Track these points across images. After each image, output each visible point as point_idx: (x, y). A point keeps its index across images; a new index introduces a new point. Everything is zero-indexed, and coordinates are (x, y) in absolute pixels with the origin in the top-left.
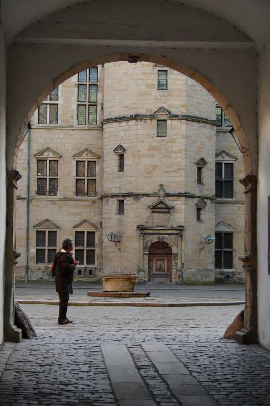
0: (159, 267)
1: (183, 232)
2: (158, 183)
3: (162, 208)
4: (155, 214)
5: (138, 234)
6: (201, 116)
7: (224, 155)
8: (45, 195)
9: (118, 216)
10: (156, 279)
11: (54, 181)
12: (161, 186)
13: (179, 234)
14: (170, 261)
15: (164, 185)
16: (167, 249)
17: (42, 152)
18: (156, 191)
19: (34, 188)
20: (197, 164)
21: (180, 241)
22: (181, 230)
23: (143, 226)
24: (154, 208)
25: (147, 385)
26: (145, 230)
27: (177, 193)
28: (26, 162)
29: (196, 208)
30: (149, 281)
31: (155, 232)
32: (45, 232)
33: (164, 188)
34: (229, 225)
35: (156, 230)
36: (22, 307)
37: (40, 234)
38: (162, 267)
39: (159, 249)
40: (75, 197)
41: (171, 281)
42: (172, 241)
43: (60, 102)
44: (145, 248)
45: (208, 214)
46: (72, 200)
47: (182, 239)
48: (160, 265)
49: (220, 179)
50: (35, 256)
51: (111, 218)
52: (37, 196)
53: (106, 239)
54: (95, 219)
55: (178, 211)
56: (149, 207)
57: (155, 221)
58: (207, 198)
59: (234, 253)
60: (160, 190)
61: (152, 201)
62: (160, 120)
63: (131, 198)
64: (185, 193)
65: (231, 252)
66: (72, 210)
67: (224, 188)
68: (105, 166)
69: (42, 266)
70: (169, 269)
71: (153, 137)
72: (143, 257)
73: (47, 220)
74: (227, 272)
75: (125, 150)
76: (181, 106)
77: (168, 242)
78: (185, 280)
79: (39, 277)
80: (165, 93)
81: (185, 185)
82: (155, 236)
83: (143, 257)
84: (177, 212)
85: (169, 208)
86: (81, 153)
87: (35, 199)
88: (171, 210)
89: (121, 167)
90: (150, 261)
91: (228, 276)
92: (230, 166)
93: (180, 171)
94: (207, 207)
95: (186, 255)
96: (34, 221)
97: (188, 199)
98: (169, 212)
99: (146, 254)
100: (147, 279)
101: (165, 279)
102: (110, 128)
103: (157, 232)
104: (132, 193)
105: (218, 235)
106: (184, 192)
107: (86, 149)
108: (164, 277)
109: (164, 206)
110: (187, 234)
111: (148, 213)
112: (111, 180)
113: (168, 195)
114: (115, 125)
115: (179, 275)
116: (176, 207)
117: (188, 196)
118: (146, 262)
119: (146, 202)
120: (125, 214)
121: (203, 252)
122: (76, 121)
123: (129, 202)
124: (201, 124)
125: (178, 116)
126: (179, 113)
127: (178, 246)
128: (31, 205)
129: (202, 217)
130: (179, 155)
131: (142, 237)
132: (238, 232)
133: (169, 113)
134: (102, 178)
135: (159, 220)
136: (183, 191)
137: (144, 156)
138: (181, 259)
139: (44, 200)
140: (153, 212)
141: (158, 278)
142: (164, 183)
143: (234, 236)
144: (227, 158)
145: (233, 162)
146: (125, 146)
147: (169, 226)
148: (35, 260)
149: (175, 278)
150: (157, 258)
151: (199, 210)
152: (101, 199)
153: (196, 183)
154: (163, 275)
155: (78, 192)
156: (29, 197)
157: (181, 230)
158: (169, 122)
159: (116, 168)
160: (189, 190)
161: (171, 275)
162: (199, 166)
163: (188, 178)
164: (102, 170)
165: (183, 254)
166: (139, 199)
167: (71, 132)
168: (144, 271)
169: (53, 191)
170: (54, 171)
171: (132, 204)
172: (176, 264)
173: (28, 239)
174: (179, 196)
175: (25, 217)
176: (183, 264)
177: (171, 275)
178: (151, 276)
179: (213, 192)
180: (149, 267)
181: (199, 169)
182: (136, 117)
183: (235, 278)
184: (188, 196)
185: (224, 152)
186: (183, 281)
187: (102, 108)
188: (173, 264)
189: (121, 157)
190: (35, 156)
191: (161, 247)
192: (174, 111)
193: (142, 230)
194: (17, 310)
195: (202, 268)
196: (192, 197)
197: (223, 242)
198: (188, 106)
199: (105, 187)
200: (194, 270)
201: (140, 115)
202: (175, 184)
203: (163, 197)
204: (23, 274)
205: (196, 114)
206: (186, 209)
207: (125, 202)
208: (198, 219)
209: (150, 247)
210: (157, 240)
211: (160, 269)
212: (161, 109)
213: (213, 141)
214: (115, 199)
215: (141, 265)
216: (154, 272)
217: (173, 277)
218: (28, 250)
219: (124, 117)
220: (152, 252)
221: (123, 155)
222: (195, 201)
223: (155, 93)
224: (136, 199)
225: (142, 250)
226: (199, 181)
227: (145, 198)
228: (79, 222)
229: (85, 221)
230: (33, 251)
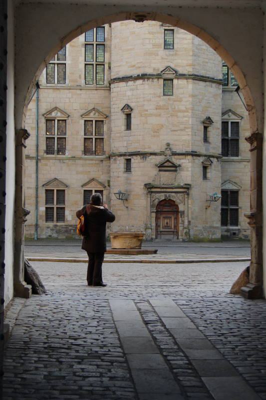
0: (166, 225)
2: (165, 142)
5: (146, 192)
6: (207, 75)
7: (230, 113)
8: (53, 154)
9: (126, 175)
10: (163, 237)
11: (62, 140)
12: (168, 145)
13: (186, 192)
14: (176, 219)
15: (171, 143)
17: (50, 112)
19: (43, 147)
20: (203, 123)
22: (188, 188)
23: (150, 184)
24: (161, 167)
25: (155, 339)
26: (152, 188)
27: (184, 151)
28: (35, 121)
30: (156, 238)
31: (162, 190)
32: (53, 190)
33: (171, 146)
34: (235, 183)
35: (163, 188)
36: (31, 264)
37: (49, 192)
39: (166, 208)
40: (84, 156)
41: (178, 238)
43: (68, 62)
44: (152, 206)
45: (214, 172)
46: (80, 159)
47: (188, 198)
48: (167, 223)
49: (226, 138)
50: (44, 214)
51: (118, 177)
52: (46, 156)
53: (113, 197)
54: (103, 178)
55: (185, 169)
56: (156, 165)
57: (162, 179)
58: (213, 157)
59: (240, 210)
61: (159, 159)
62: (167, 79)
63: (139, 157)
64: (192, 152)
65: (237, 210)
66: (80, 169)
67: (230, 146)
68: (113, 125)
69: (51, 224)
70: (176, 227)
71: (160, 97)
72: (151, 215)
73: (56, 179)
74: (233, 230)
75: (132, 110)
76: (187, 66)
77: (174, 200)
78: (192, 237)
79: (48, 235)
80: (171, 52)
82: (163, 194)
84: (183, 170)
85: (176, 167)
86: (89, 112)
87: (43, 158)
88: (178, 168)
89: (128, 126)
90: (157, 218)
91: (234, 234)
92: (236, 125)
93: (187, 130)
94: (213, 166)
95: (192, 213)
96: (43, 179)
97: (195, 158)
98: (176, 171)
99: (152, 212)
100: (154, 237)
101: (172, 236)
102: (117, 88)
103: (165, 190)
104: (139, 152)
105: (224, 192)
106: (190, 151)
107: (94, 109)
108: (171, 234)
109: (170, 164)
110: (194, 192)
111: (155, 171)
112: (118, 139)
114: (122, 84)
115: (186, 233)
116: (183, 165)
117: (194, 154)
118: (154, 220)
119: (153, 161)
120: (133, 173)
121: (209, 210)
122: (83, 81)
123: (137, 161)
124: (207, 83)
125: (185, 75)
126: (185, 72)
127: (184, 204)
128: (40, 164)
129: (209, 175)
130: (186, 114)
131: (149, 196)
132: (244, 190)
133: (176, 72)
134: (110, 137)
135: (166, 178)
136: (189, 149)
137: (151, 115)
139: (52, 159)
140: (160, 171)
142: (171, 142)
143: (240, 193)
144: (233, 117)
145: (239, 121)
146: (132, 105)
147: (176, 184)
148: (44, 218)
149: (182, 235)
150: (164, 215)
151: (205, 168)
152: (109, 158)
154: (171, 233)
155: (86, 151)
156: (37, 156)
157: (188, 188)
158: (175, 81)
159: (123, 128)
161: (178, 232)
162: (205, 125)
163: (194, 136)
164: (110, 129)
165: (190, 212)
166: (146, 158)
167: (79, 92)
168: (151, 229)
169: (61, 150)
170: (62, 130)
171: (139, 162)
172: (183, 221)
173: (37, 197)
174: (186, 154)
175: (34, 176)
176: (189, 222)
177: (177, 232)
178: (158, 233)
179: (220, 151)
180: (156, 224)
181: (206, 128)
182: (143, 77)
183: (241, 236)
184: (194, 154)
185: (230, 110)
187: (110, 68)
188: (180, 221)
189: (129, 116)
190: (43, 115)
191: (167, 205)
192: (181, 71)
193: (149, 188)
194: (26, 267)
195: (208, 225)
196: (199, 156)
197: (229, 200)
198: (194, 65)
199: (112, 146)
200: (200, 227)
201: (146, 75)
203: (170, 156)
204: (33, 232)
205: (202, 73)
207: (132, 161)
208: (205, 177)
209: (157, 205)
211: (167, 226)
212: (168, 68)
213: (220, 100)
214: (122, 158)
215: (149, 223)
216: (161, 229)
217: (180, 234)
218: (37, 208)
219: (131, 77)
220: (159, 210)
221: (130, 114)
222: (202, 159)
223: (162, 52)
225: (149, 208)
226: (206, 139)
227: (152, 157)
228: (88, 180)
229: (93, 179)
230: (42, 209)
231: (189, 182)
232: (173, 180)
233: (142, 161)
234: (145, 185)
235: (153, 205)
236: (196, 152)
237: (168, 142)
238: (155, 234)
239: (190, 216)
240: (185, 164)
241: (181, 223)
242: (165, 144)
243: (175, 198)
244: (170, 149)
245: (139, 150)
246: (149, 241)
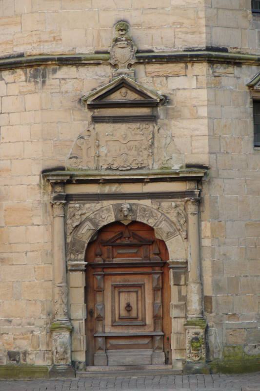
0: (123, 313)
1: (205, 188)
2: (111, 18)
3: (122, 102)
4: (101, 127)
5: (48, 199)
10: (116, 357)
12: (123, 26)
13: (190, 193)
14: (161, 289)
15: (132, 21)
16: (154, 249)
18: (106, 45)
21: (192, 220)
22: (198, 180)
23: (63, 169)
24: (100, 105)
26: (69, 182)
27: (179, 48)
29: (249, 100)
30: (90, 362)
31: (107, 189)
33: (133, 32)
34: (99, 64)
38: (134, 314)
41: (167, 361)
44: (69, 248)
47: (199, 214)
48: (128, 307)
55: (186, 112)
56: (82, 101)
57: (103, 150)
60: (116, 40)
61: (92, 80)
64: (208, 49)
70: (160, 318)
77: (151, 222)
81: (208, 19)
82: (107, 204)
83: (67, 282)
84: (179, 116)
85: (153, 105)
88: (160, 110)
95: (217, 269)
97: (220, 69)
98: (153, 119)
99: (76, 269)
100: (81, 358)
101: (149, 352)
104: (22, 55)
108: (145, 346)
109: (132, 96)
111: (78, 122)
113: (146, 58)
115: (196, 339)
116: (178, 98)
117: (217, 57)
118: (78, 295)
119: (69, 86)
127: (186, 238)
131: (58, 211)
135: (117, 145)
136: (199, 41)
140: (96, 120)
141: (124, 352)
142: (133, 18)
147: (156, 167)
149: (181, 350)
150: (118, 280)
153: (249, 12)
154: (146, 341)
157: (198, 180)
160: (221, 39)
161: (169, 339)
165: (207, 264)
166: (44, 76)
168: (71, 331)
172: (183, 298)
176: (206, 301)
178: (97, 343)
184: (217, 57)
186: (208, 362)
191: (126, 241)
193: (61, 182)
196: (236, 62)
202: (172, 19)
203: (130, 65)
206: (212, 103)
209: (90, 244)
210: (112, 219)
211: (129, 318)
215: (60, 308)
216: (109, 330)
217: (173, 345)
220: (99, 260)
224: (35, 76)
227: (66, 72)
231: (202, 158)
232: (146, 153)
233: (31, 86)
234: (44, 172)
235: (73, 244)
236: (225, 50)
237: (122, 16)
238: (83, 347)
239: (208, 279)
240: (186, 93)
241: (176, 306)
242: (112, 21)
243: (152, 215)
244: (130, 41)
245: (18, 50)
246: (64, 373)
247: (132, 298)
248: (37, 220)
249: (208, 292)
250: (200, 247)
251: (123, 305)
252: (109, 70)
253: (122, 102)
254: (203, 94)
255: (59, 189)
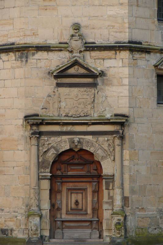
0: (73, 206)
2: (69, 22)
3: (75, 75)
4: (64, 91)
5: (28, 134)
10: (68, 233)
12: (77, 27)
14: (97, 192)
15: (82, 24)
16: (93, 166)
18: (66, 38)
21: (118, 149)
22: (122, 124)
23: (37, 115)
24: (61, 76)
26: (41, 124)
27: (111, 41)
29: (155, 75)
30: (52, 236)
31: (65, 129)
33: (83, 31)
34: (61, 50)
35: (66, 125)
38: (80, 207)
41: (100, 237)
42: (102, 148)
44: (40, 165)
47: (122, 145)
48: (77, 203)
55: (115, 82)
56: (50, 73)
57: (63, 104)
60: (73, 36)
64: (129, 42)
70: (97, 210)
72: (39, 185)
77: (92, 150)
81: (130, 24)
82: (65, 138)
83: (39, 185)
84: (110, 84)
85: (94, 76)
88: (99, 80)
90: (53, 192)
95: (132, 180)
97: (137, 55)
99: (44, 178)
100: (47, 233)
101: (89, 231)
103: (69, 128)
104: (13, 44)
106: (127, 40)
109: (82, 71)
111: (47, 87)
115: (118, 224)
116: (110, 73)
117: (135, 48)
118: (46, 195)
119: (42, 64)
127: (114, 160)
131: (34, 141)
135: (72, 101)
136: (124, 37)
138: (122, 187)
140: (59, 85)
141: (73, 231)
142: (83, 22)
147: (96, 116)
149: (109, 230)
150: (71, 185)
153: (156, 19)
154: (87, 224)
157: (122, 124)
160: (138, 36)
161: (101, 223)
163: (135, 8)
165: (126, 176)
166: (27, 57)
168: (41, 217)
171: (12, 68)
172: (111, 198)
176: (125, 200)
177: (100, 223)
178: (56, 225)
184: (135, 48)
186: (126, 237)
188: (106, 199)
191: (76, 161)
196: (147, 51)
202: (107, 23)
203: (81, 52)
206: (131, 76)
209: (53, 163)
210: (68, 147)
211: (77, 210)
215: (34, 202)
216: (64, 217)
220: (59, 173)
224: (21, 57)
227: (40, 55)
231: (125, 111)
232: (89, 106)
233: (19, 63)
234: (26, 117)
235: (43, 162)
236: (140, 43)
237: (77, 20)
238: (48, 227)
240: (116, 69)
241: (107, 203)
243: (92, 145)
244: (81, 37)
245: (11, 40)
247: (79, 197)
248: (20, 147)
249: (127, 194)
250: (122, 166)
251: (73, 201)
252: (67, 54)
253: (75, 75)
254: (126, 71)
255: (34, 128)
